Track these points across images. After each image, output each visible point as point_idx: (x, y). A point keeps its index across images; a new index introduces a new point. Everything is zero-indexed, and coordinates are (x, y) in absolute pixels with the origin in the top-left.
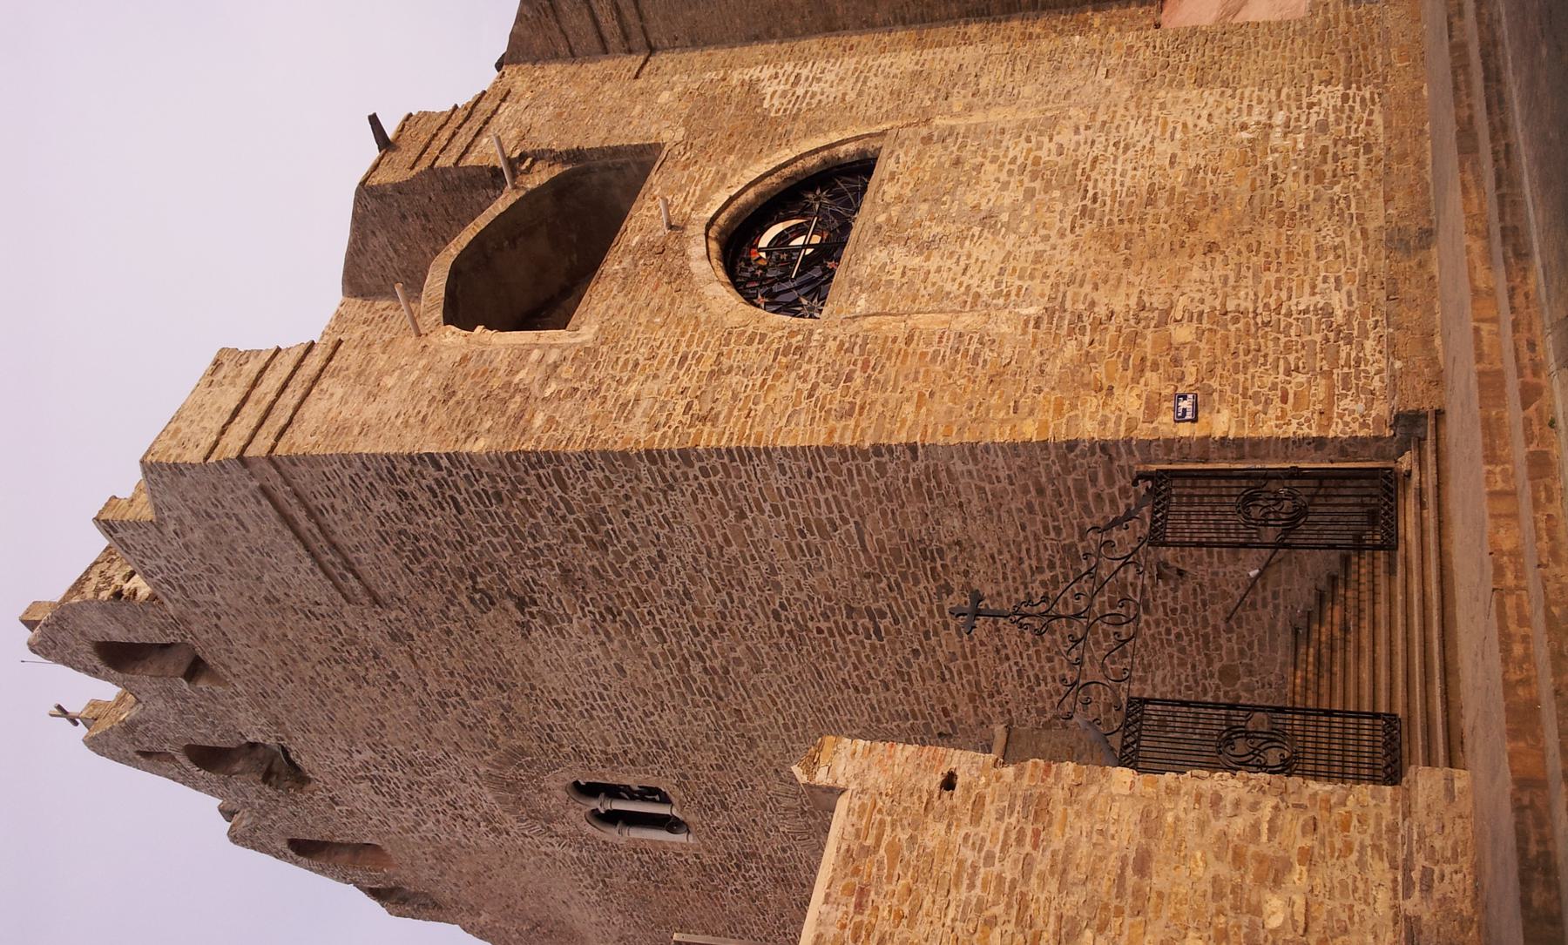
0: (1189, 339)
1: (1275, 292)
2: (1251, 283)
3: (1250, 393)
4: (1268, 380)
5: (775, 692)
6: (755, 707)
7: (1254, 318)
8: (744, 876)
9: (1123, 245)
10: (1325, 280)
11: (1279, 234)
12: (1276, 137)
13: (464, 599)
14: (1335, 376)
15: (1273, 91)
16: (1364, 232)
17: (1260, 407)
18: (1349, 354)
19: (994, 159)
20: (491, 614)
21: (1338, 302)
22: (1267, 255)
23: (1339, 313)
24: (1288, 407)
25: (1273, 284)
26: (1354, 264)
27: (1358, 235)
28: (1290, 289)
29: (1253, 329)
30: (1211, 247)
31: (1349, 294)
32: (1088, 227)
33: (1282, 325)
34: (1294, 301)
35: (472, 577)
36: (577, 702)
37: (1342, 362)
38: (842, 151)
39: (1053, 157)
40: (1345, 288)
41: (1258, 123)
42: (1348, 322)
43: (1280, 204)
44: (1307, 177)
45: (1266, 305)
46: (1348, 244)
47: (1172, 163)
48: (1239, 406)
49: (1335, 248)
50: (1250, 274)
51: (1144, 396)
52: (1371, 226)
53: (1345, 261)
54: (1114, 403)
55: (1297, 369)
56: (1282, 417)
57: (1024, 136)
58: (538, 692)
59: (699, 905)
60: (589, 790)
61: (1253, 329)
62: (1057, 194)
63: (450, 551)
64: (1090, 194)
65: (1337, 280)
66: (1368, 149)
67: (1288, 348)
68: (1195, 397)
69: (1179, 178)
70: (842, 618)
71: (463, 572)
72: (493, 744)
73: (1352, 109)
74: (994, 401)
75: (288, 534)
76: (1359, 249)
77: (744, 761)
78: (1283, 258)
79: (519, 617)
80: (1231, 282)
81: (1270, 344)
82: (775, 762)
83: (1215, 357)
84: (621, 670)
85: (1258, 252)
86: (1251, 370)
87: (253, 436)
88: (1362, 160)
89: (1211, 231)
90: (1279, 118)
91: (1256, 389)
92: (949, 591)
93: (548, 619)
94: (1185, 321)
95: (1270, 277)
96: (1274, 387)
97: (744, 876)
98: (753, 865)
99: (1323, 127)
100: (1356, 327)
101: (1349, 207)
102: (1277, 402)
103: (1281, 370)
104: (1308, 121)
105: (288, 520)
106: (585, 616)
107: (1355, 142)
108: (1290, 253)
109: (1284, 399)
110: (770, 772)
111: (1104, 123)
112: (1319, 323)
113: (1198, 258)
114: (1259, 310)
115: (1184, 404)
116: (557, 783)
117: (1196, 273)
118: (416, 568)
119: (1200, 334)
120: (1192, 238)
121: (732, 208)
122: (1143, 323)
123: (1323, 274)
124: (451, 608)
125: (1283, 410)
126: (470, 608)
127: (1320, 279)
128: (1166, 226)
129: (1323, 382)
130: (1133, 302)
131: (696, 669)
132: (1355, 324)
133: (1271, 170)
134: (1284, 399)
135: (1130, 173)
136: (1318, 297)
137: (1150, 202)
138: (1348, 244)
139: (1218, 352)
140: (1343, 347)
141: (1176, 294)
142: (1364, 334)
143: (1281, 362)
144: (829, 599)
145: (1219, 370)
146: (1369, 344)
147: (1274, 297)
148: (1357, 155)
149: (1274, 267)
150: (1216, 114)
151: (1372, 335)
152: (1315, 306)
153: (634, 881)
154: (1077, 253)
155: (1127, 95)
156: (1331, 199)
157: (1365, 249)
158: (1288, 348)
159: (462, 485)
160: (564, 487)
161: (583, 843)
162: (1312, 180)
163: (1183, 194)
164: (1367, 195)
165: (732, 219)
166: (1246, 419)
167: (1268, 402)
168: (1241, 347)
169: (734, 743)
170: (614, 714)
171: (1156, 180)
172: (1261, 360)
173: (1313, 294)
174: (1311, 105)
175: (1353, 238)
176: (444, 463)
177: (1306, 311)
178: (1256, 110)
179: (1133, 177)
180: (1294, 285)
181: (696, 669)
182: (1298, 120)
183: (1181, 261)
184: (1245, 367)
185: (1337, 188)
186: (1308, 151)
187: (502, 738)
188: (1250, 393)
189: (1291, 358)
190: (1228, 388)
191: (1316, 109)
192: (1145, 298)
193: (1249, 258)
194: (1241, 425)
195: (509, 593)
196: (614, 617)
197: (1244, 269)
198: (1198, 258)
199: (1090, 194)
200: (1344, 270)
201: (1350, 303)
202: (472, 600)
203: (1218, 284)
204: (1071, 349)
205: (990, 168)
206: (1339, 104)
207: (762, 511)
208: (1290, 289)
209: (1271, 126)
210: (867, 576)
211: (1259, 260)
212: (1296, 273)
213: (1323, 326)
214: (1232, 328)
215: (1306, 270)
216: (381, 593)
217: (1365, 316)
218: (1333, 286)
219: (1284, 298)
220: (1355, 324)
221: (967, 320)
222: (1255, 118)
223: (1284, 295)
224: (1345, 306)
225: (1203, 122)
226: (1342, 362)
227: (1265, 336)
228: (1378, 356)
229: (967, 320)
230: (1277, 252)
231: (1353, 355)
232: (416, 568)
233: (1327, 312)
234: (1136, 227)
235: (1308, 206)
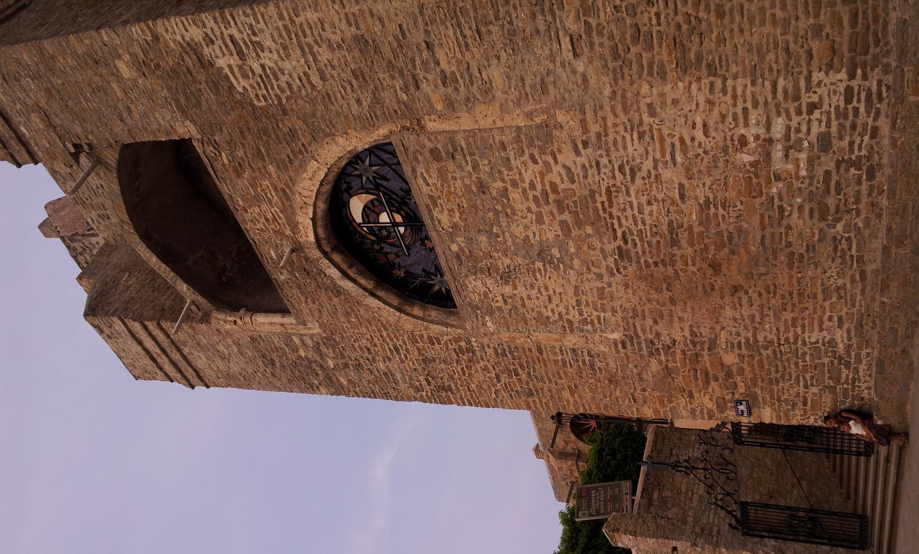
0: (735, 361)
1: (792, 329)
2: (772, 320)
3: (782, 399)
4: (793, 392)
7: (779, 347)
9: (664, 287)
10: (830, 319)
11: (791, 277)
14: (838, 390)
15: (767, 83)
16: (863, 274)
17: (790, 407)
18: (847, 376)
21: (840, 336)
22: (783, 297)
23: (841, 346)
24: (808, 407)
26: (853, 305)
27: (858, 277)
28: (803, 326)
29: (779, 356)
30: (736, 289)
31: (849, 331)
32: (630, 269)
33: (800, 352)
34: (806, 335)
37: (843, 381)
40: (846, 326)
41: (757, 137)
42: (848, 353)
43: (789, 245)
44: (811, 211)
45: (787, 340)
46: (849, 286)
47: (682, 197)
48: (777, 407)
49: (838, 288)
50: (771, 313)
51: (714, 399)
52: (870, 268)
53: (846, 302)
54: (697, 402)
55: (812, 385)
56: (804, 415)
61: (779, 356)
62: (589, 230)
64: (619, 234)
65: (840, 319)
66: (871, 176)
67: (805, 369)
68: (747, 402)
73: (856, 110)
74: (618, 393)
76: (858, 291)
78: (796, 298)
80: (758, 319)
81: (793, 366)
83: (755, 374)
85: (775, 294)
86: (781, 384)
88: (864, 187)
91: (785, 397)
94: (729, 349)
95: (788, 316)
96: (798, 395)
99: (825, 142)
100: (853, 357)
101: (850, 250)
102: (800, 404)
103: (802, 384)
104: (809, 132)
107: (857, 164)
108: (801, 295)
109: (805, 404)
111: (599, 135)
112: (826, 351)
113: (727, 299)
114: (782, 342)
115: (741, 408)
117: (728, 312)
119: (741, 357)
120: (719, 282)
121: (320, 223)
122: (699, 347)
123: (828, 314)
125: (805, 410)
127: (826, 316)
128: (694, 269)
129: (830, 396)
130: (687, 333)
132: (853, 354)
133: (776, 200)
134: (805, 404)
135: (647, 209)
136: (825, 333)
137: (674, 242)
138: (849, 286)
139: (757, 372)
140: (843, 370)
141: (718, 328)
142: (859, 360)
143: (801, 378)
145: (760, 383)
146: (862, 367)
148: (859, 183)
149: (789, 307)
150: (711, 122)
151: (864, 362)
152: (823, 340)
154: (630, 291)
156: (835, 238)
157: (863, 291)
158: (805, 369)
162: (816, 214)
163: (700, 234)
164: (867, 233)
165: (325, 228)
166: (782, 414)
167: (794, 405)
168: (773, 369)
171: (673, 216)
172: (787, 377)
174: (812, 107)
175: (853, 280)
177: (817, 342)
178: (753, 117)
180: (806, 322)
182: (798, 130)
183: (715, 300)
184: (777, 382)
185: (840, 227)
186: (811, 178)
188: (782, 399)
189: (808, 376)
190: (767, 395)
191: (817, 114)
192: (695, 330)
193: (768, 300)
194: (778, 417)
197: (766, 309)
198: (727, 299)
199: (619, 234)
200: (845, 310)
201: (850, 339)
203: (747, 321)
204: (654, 365)
206: (842, 104)
208: (803, 326)
209: (770, 141)
211: (776, 302)
212: (807, 312)
213: (829, 354)
215: (815, 309)
217: (860, 348)
218: (836, 324)
219: (800, 333)
220: (853, 354)
221: (572, 340)
222: (754, 131)
223: (799, 330)
224: (846, 340)
225: (699, 134)
226: (843, 381)
227: (788, 360)
228: (867, 378)
229: (572, 340)
230: (791, 293)
231: (850, 377)
233: (832, 343)
234: (670, 270)
235: (814, 247)
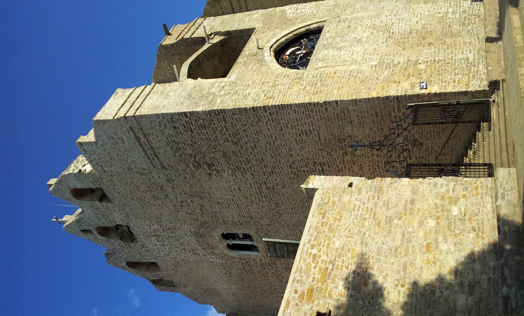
0: (424, 68)
1: (451, 55)
2: (443, 53)
3: (444, 81)
4: (449, 77)
5: (289, 196)
6: (282, 202)
8: (275, 267)
9: (402, 44)
10: (466, 51)
11: (452, 40)
12: (450, 15)
13: (191, 166)
14: (470, 75)
15: (448, 3)
16: (478, 38)
17: (447, 84)
18: (474, 70)
19: (361, 25)
20: (199, 170)
21: (471, 57)
22: (448, 45)
24: (456, 84)
25: (450, 52)
26: (475, 46)
27: (477, 39)
28: (455, 54)
30: (430, 44)
31: (474, 54)
33: (453, 63)
34: (457, 56)
35: (195, 157)
36: (225, 202)
38: (312, 27)
39: (379, 24)
40: (473, 53)
41: (444, 12)
43: (452, 32)
44: (460, 25)
46: (473, 41)
48: (440, 84)
49: (469, 42)
50: (442, 50)
51: (410, 83)
52: (480, 36)
53: (473, 45)
54: (400, 86)
55: (458, 74)
56: (454, 86)
57: (370, 19)
58: (213, 199)
59: (260, 279)
60: (226, 236)
61: (444, 65)
62: (381, 33)
63: (188, 148)
64: (391, 32)
65: (470, 51)
66: (479, 17)
67: (455, 69)
68: (426, 83)
69: (419, 27)
70: (311, 166)
71: (192, 155)
72: (197, 220)
73: (474, 7)
74: (362, 87)
75: (138, 144)
76: (477, 42)
77: (278, 222)
78: (453, 46)
79: (208, 171)
80: (437, 52)
81: (450, 68)
82: (288, 222)
83: (432, 72)
84: (239, 189)
85: (445, 44)
86: (444, 75)
87: (128, 110)
88: (477, 20)
89: (430, 40)
90: (451, 10)
91: (445, 80)
92: (347, 154)
93: (218, 172)
94: (422, 64)
95: (449, 51)
96: (451, 79)
97: (275, 267)
98: (279, 263)
99: (464, 12)
101: (473, 32)
102: (452, 83)
104: (460, 10)
105: (138, 139)
106: (229, 170)
107: (475, 15)
108: (455, 44)
109: (454, 82)
110: (286, 226)
111: (395, 14)
112: (465, 62)
113: (426, 47)
115: (422, 84)
116: (217, 234)
117: (425, 51)
118: (177, 154)
119: (427, 67)
120: (424, 42)
121: (278, 43)
122: (409, 65)
123: (466, 49)
124: (187, 169)
125: (454, 85)
126: (193, 168)
127: (465, 50)
128: (416, 39)
129: (467, 77)
130: (406, 59)
131: (264, 187)
132: (476, 62)
133: (448, 24)
134: (454, 82)
135: (404, 26)
136: (464, 55)
138: (473, 41)
139: (433, 71)
141: (419, 57)
142: (479, 63)
144: (308, 159)
145: (433, 75)
146: (481, 67)
147: (450, 56)
148: (475, 18)
149: (450, 48)
150: (430, 10)
151: (481, 64)
153: (239, 271)
154: (388, 48)
155: (402, 6)
156: (468, 30)
157: (479, 42)
158: (455, 69)
159: (194, 123)
160: (225, 122)
161: (223, 256)
162: (461, 25)
163: (421, 31)
164: (479, 28)
165: (278, 46)
166: (442, 88)
167: (449, 83)
168: (440, 69)
169: (275, 216)
170: (236, 206)
171: (412, 28)
173: (463, 54)
174: (460, 7)
175: (475, 39)
176: (189, 115)
178: (443, 8)
179: (405, 27)
180: (457, 52)
181: (264, 187)
182: (456, 10)
183: (421, 48)
184: (442, 74)
185: (470, 27)
186: (460, 18)
187: (200, 217)
188: (444, 81)
191: (462, 7)
192: (410, 58)
193: (442, 46)
194: (441, 89)
195: (206, 162)
196: (239, 170)
197: (441, 49)
198: (426, 47)
199: (391, 32)
200: (472, 48)
201: (474, 56)
202: (194, 165)
203: (433, 53)
204: (386, 72)
205: (359, 28)
206: (469, 5)
207: (288, 128)
208: (455, 54)
209: (448, 12)
210: (320, 150)
211: (446, 47)
214: (437, 65)
215: (460, 49)
216: (165, 164)
217: (479, 59)
220: (476, 62)
221: (353, 67)
222: (443, 10)
223: (453, 55)
224: (473, 57)
225: (427, 12)
227: (448, 66)
228: (483, 69)
229: (353, 67)
230: (451, 44)
231: (476, 69)
232: (177, 154)
233: (467, 59)
234: (406, 40)
235: (460, 32)
